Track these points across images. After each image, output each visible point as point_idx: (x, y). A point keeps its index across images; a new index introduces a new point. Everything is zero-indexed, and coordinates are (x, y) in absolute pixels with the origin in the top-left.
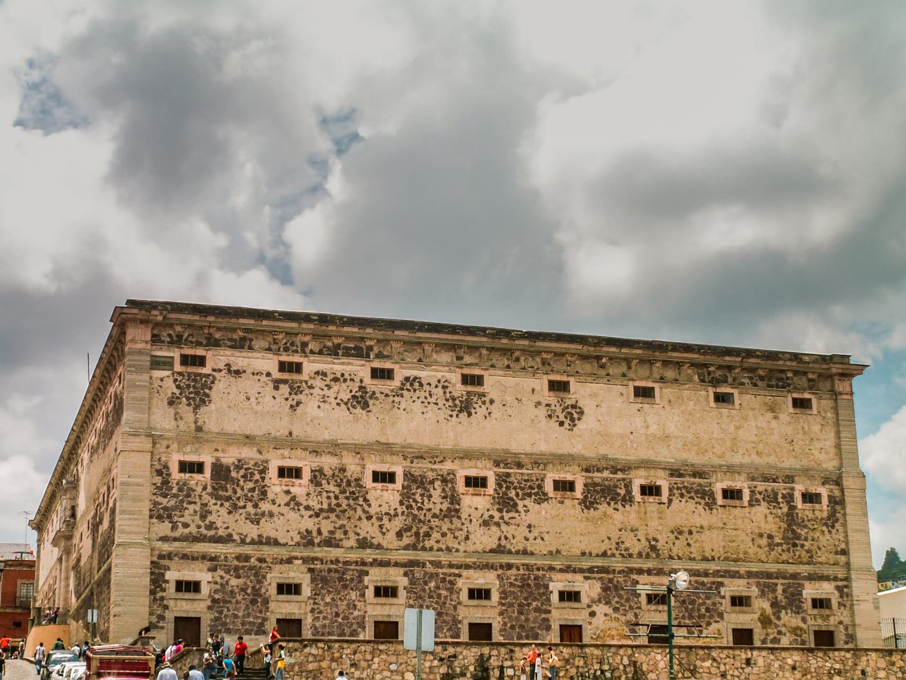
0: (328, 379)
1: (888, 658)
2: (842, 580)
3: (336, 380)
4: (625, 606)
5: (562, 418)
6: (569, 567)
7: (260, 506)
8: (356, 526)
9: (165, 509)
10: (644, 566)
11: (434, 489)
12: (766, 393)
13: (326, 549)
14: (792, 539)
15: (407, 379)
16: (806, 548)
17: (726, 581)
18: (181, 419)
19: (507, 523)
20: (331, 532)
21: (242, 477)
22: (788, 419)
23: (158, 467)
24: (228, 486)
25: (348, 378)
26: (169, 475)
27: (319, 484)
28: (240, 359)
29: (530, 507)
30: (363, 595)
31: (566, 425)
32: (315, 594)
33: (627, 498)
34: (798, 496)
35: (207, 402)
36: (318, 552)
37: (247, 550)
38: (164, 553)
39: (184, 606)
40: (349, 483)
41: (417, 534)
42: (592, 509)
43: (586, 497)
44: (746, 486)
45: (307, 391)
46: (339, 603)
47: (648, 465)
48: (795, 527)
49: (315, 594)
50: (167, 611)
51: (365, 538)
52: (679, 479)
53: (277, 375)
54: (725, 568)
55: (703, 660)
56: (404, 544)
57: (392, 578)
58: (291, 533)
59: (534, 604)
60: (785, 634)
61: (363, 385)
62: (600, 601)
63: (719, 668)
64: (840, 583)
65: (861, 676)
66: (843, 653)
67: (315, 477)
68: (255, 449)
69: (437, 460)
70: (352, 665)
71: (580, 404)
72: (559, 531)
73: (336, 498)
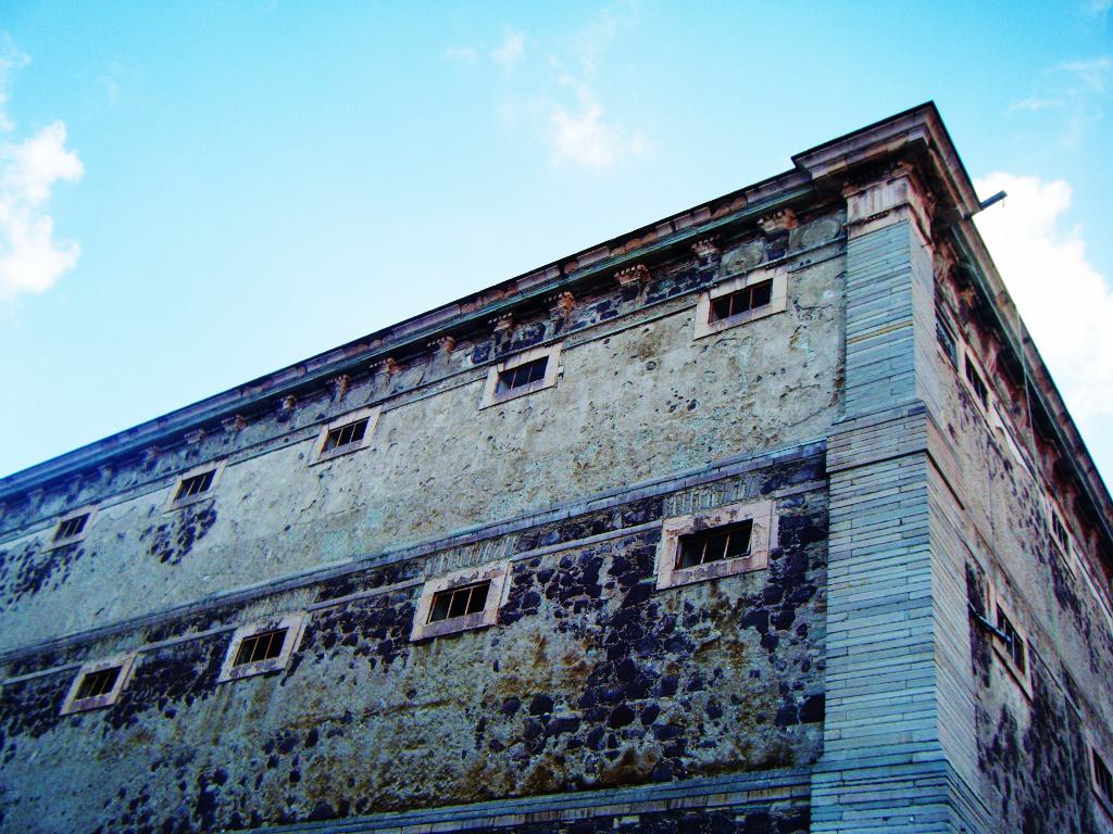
16: (662, 720)
48: (634, 656)
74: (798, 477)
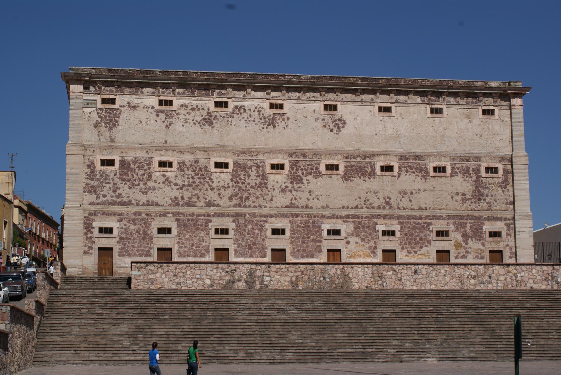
0: (189, 109)
1: (506, 269)
2: (509, 220)
3: (193, 109)
4: (368, 238)
5: (332, 127)
6: (334, 215)
7: (148, 184)
8: (204, 194)
9: (92, 187)
10: (381, 214)
11: (252, 171)
12: (465, 107)
13: (187, 207)
14: (478, 196)
15: (236, 107)
16: (487, 201)
17: (434, 222)
18: (102, 135)
19: (296, 190)
20: (190, 198)
21: (137, 168)
22: (479, 122)
23: (88, 163)
24: (129, 173)
25: (201, 108)
26: (94, 167)
27: (182, 170)
28: (136, 100)
29: (311, 181)
30: (208, 234)
31: (335, 131)
32: (180, 234)
33: (372, 174)
34: (483, 170)
35: (117, 126)
36: (182, 209)
37: (140, 209)
38: (92, 212)
39: (105, 242)
40: (200, 169)
41: (241, 198)
42: (349, 181)
43: (346, 174)
44: (449, 164)
45: (176, 117)
46: (194, 238)
47: (385, 154)
48: (480, 189)
49: (180, 234)
50: (94, 244)
51: (210, 201)
52: (405, 161)
53: (158, 107)
54: (433, 214)
55: (387, 271)
56: (233, 204)
57: (226, 224)
58: (166, 199)
59: (312, 237)
60: (470, 253)
61: (210, 112)
62: (353, 235)
63: (397, 275)
64: (508, 222)
65: (488, 279)
66: (477, 266)
67: (180, 166)
68: (145, 151)
69: (254, 154)
70: (174, 276)
71: (344, 118)
72: (328, 194)
73: (193, 178)
74: (505, 161)
